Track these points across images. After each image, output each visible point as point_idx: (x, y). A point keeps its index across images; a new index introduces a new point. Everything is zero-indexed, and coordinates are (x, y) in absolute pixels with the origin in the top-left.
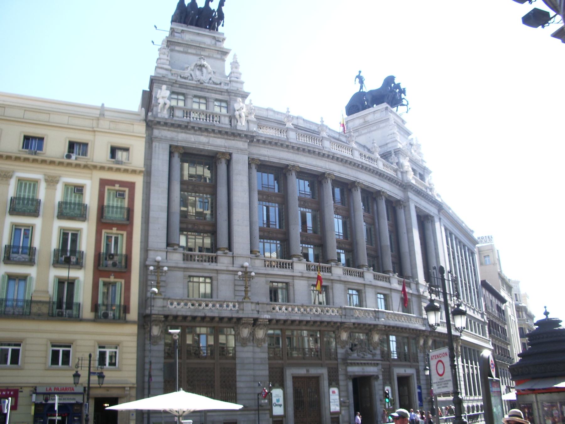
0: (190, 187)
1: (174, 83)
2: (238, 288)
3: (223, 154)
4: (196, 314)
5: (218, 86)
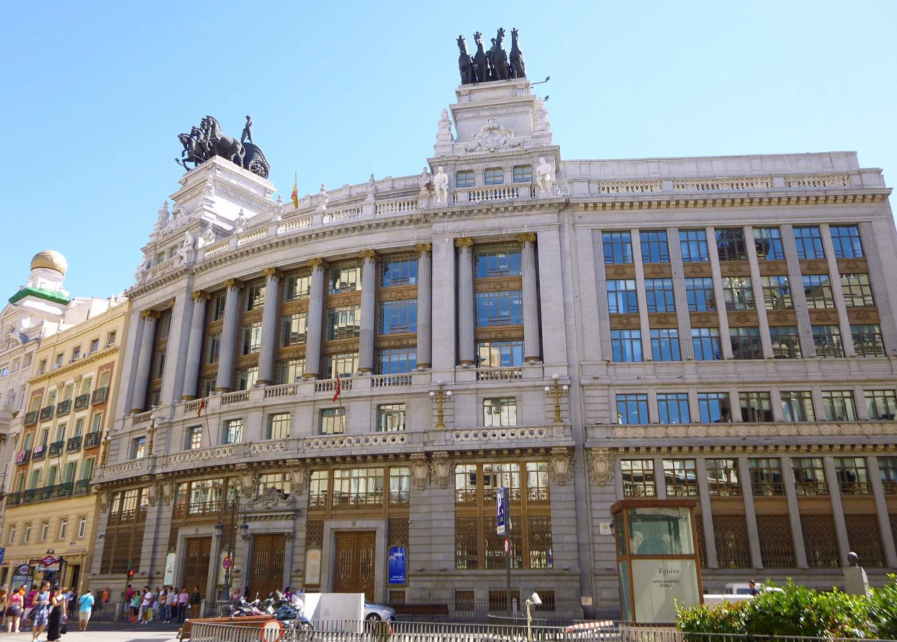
0: (492, 286)
2: (450, 412)
3: (527, 234)
4: (488, 447)
5: (516, 149)
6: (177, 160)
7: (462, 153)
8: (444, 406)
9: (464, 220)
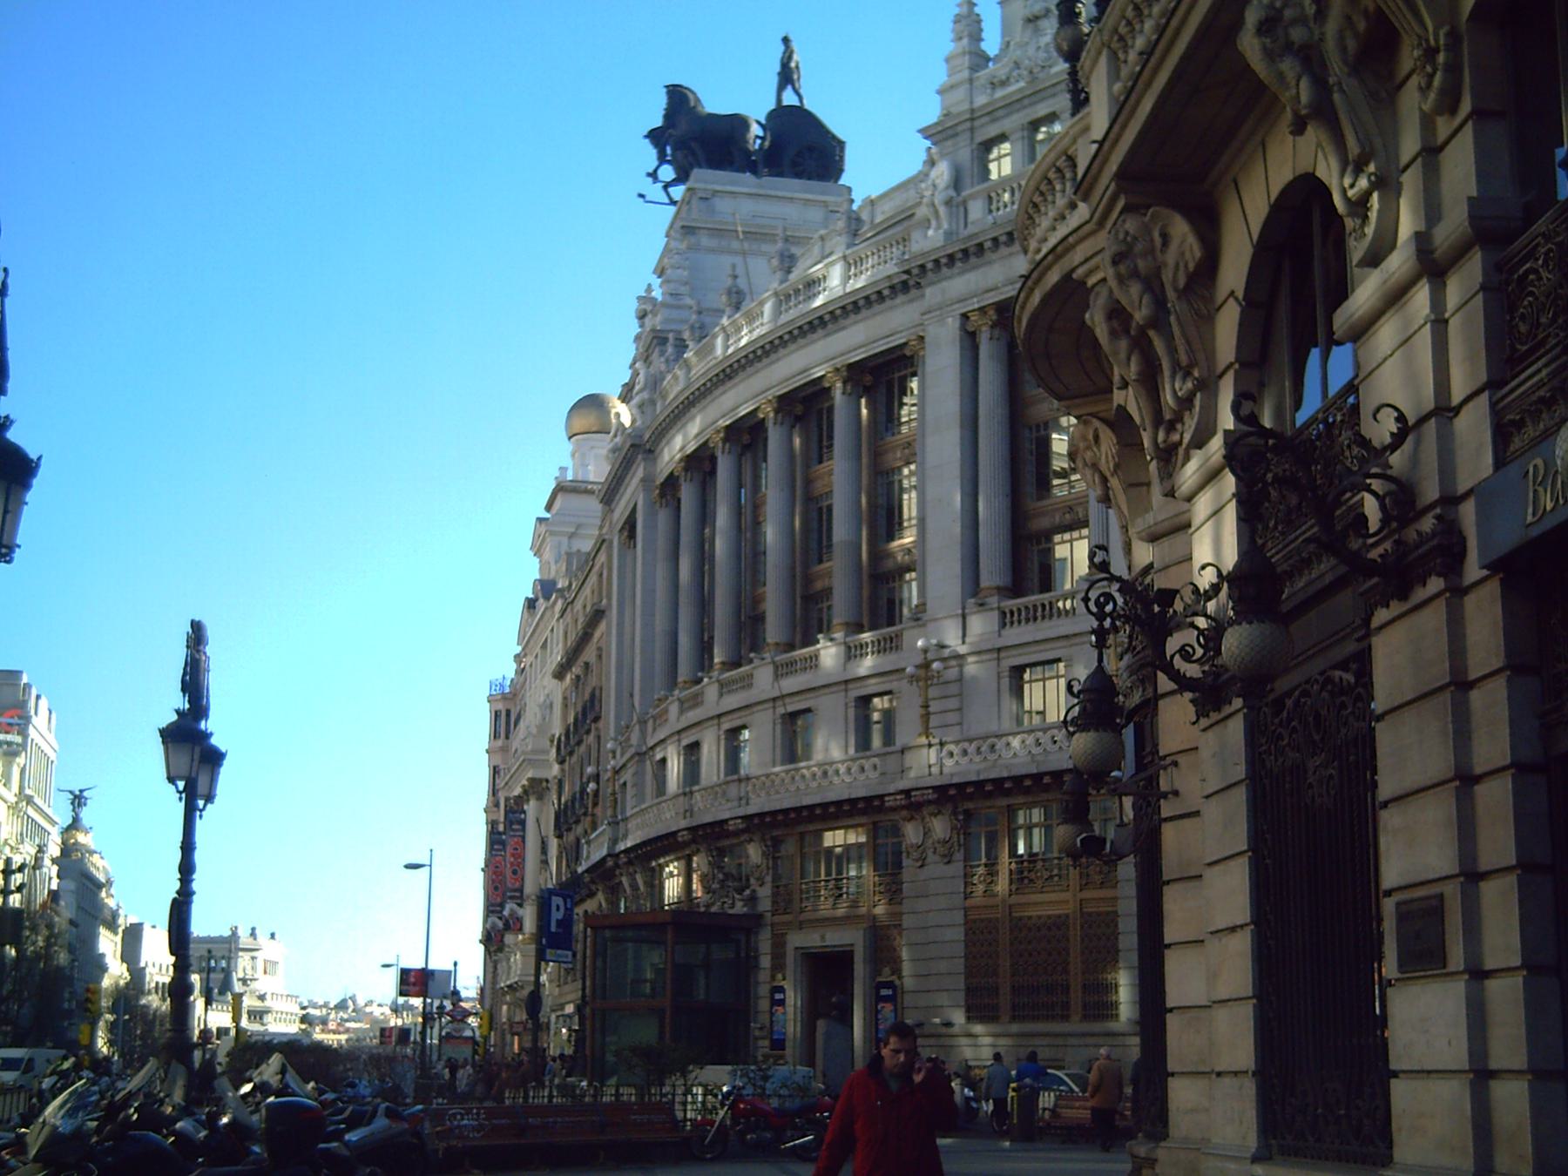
1: (972, 119)
6: (641, 196)
7: (981, 100)
8: (932, 692)
9: (975, 268)
